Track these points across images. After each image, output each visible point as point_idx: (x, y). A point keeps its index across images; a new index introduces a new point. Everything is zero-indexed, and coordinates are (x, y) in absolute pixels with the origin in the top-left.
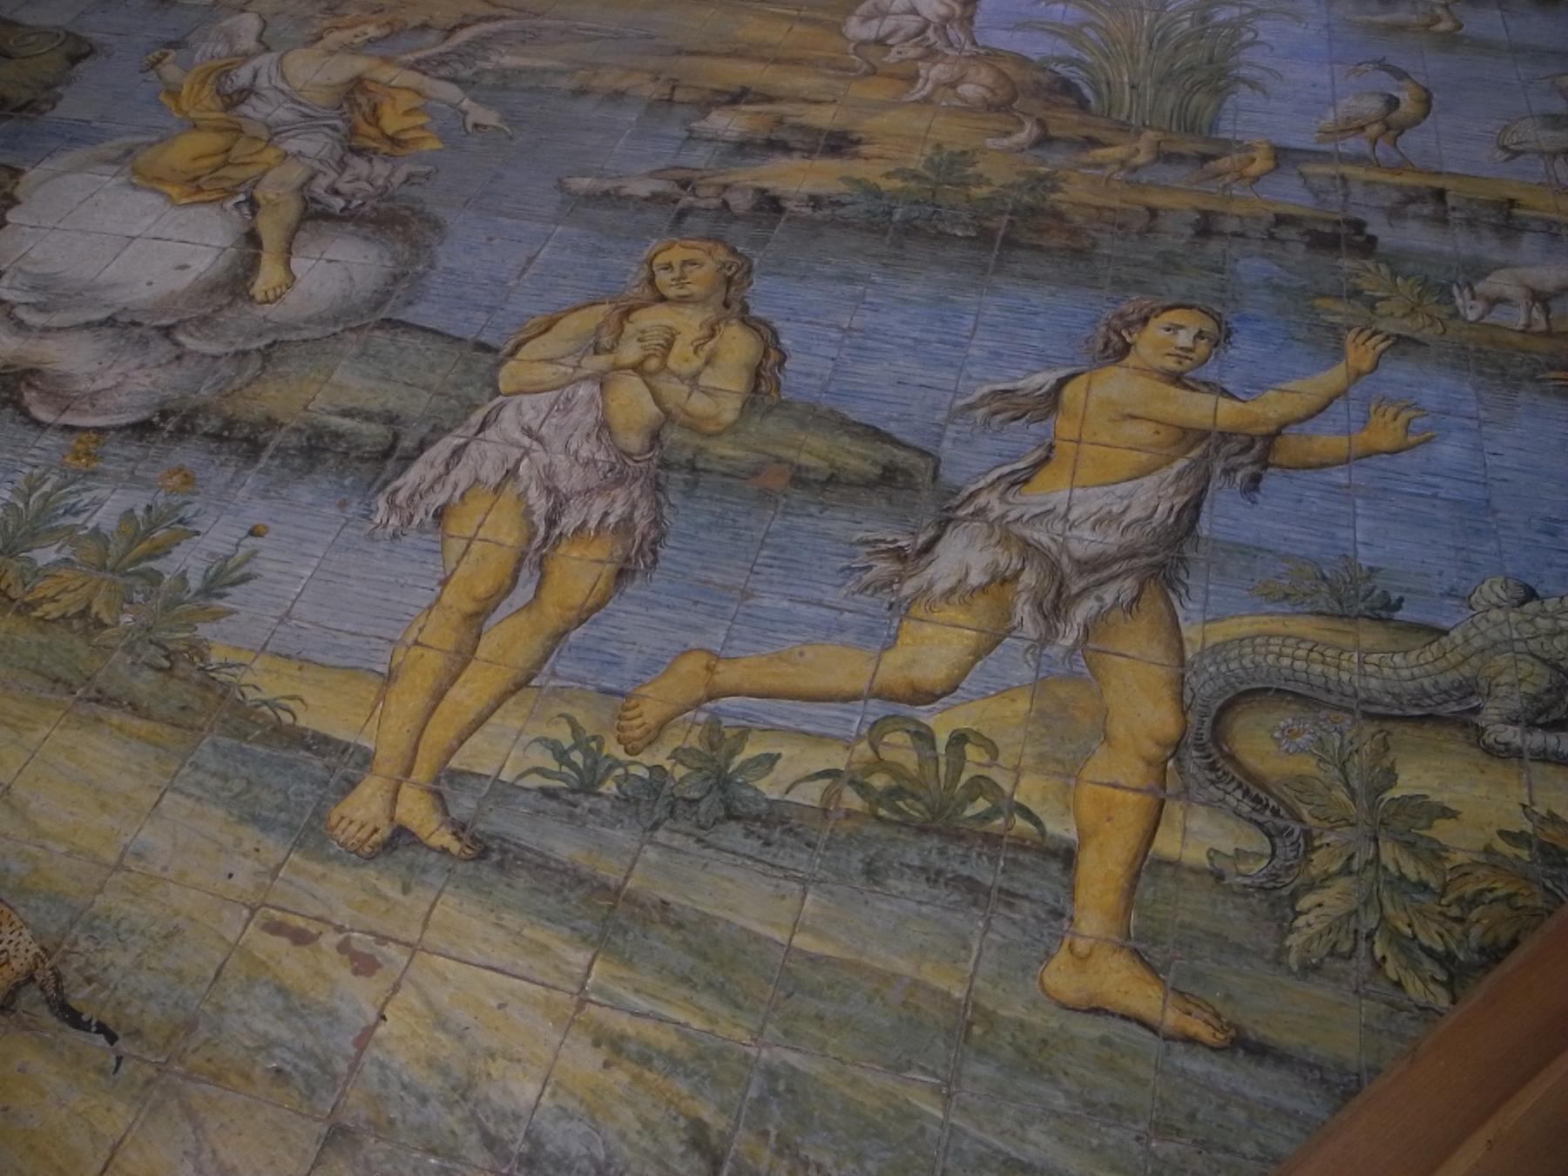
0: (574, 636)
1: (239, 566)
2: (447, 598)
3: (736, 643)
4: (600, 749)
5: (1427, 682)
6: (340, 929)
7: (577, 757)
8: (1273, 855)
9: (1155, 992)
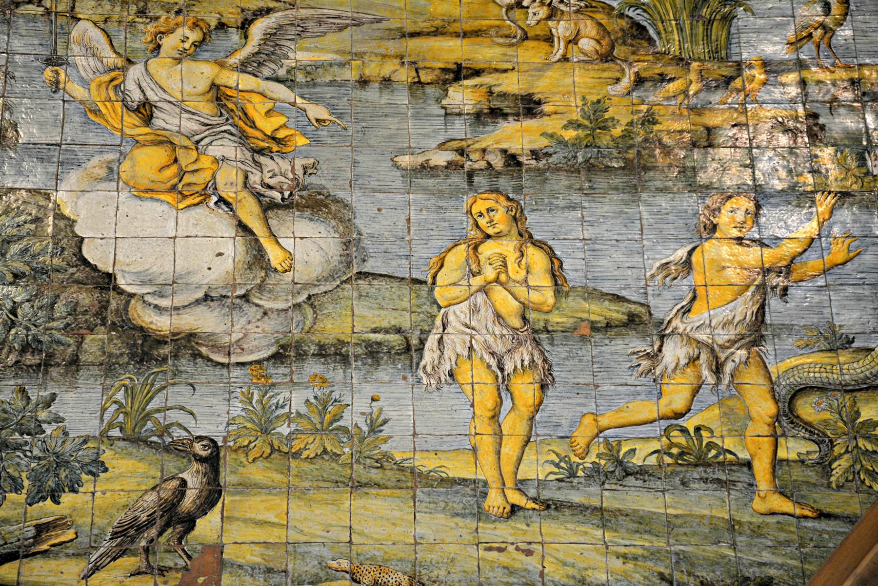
0: (538, 417)
1: (378, 417)
2: (478, 412)
3: (601, 408)
5: (868, 373)
6: (512, 544)
7: (563, 464)
8: (820, 451)
9: (790, 504)
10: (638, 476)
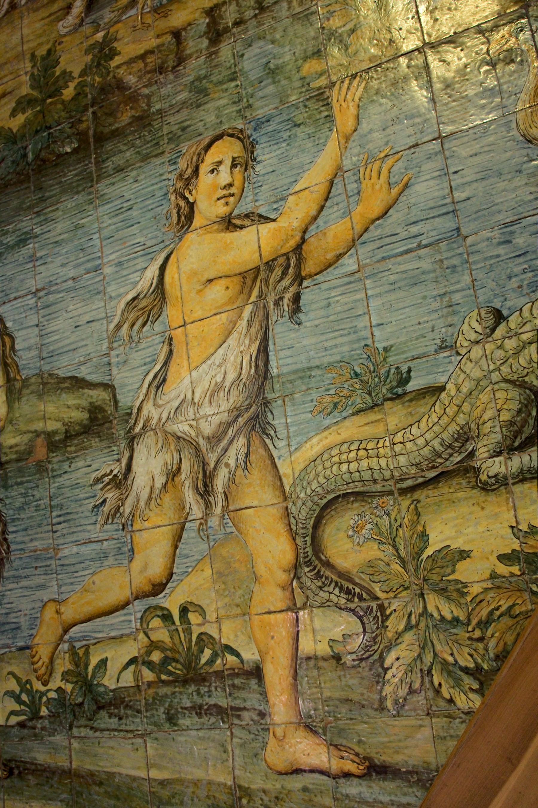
3: (63, 589)
4: (32, 687)
7: (24, 697)
10: (113, 710)
